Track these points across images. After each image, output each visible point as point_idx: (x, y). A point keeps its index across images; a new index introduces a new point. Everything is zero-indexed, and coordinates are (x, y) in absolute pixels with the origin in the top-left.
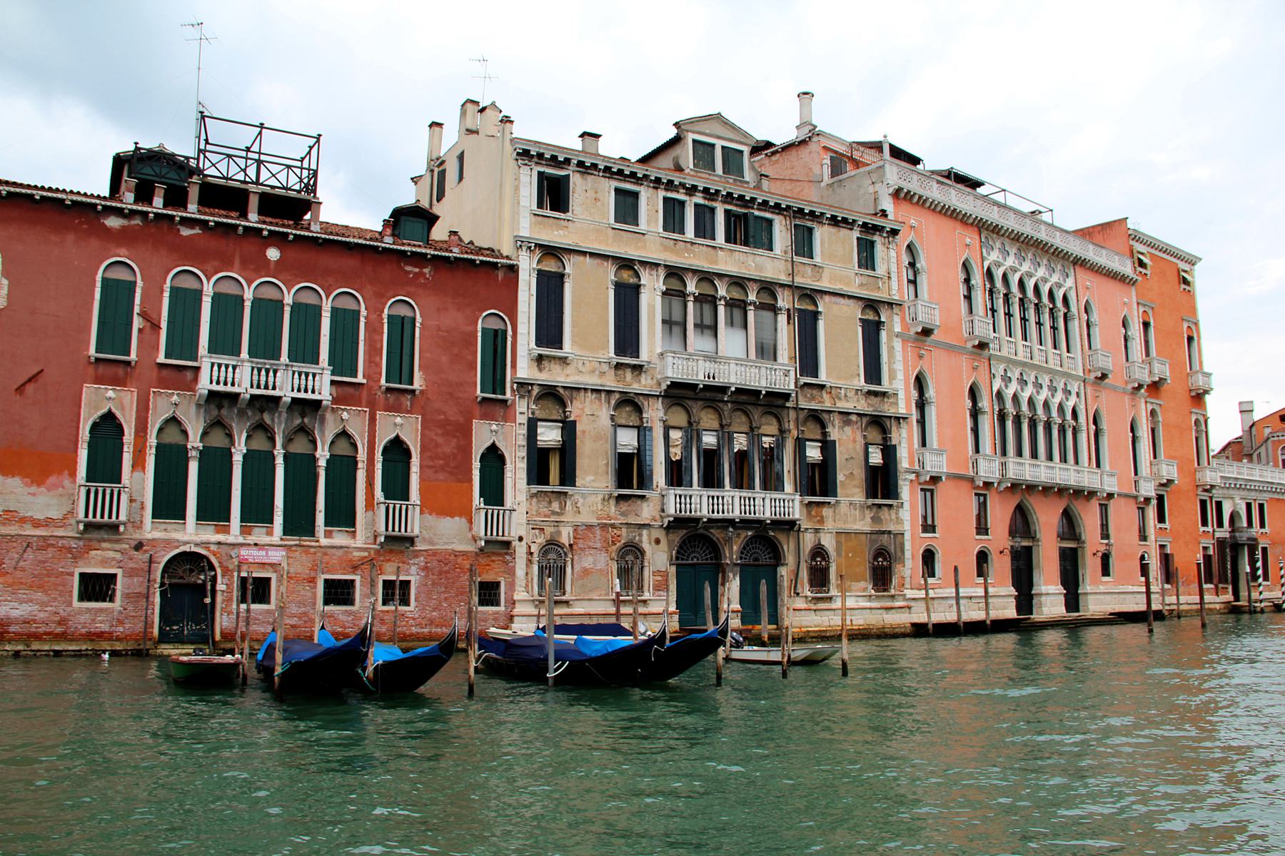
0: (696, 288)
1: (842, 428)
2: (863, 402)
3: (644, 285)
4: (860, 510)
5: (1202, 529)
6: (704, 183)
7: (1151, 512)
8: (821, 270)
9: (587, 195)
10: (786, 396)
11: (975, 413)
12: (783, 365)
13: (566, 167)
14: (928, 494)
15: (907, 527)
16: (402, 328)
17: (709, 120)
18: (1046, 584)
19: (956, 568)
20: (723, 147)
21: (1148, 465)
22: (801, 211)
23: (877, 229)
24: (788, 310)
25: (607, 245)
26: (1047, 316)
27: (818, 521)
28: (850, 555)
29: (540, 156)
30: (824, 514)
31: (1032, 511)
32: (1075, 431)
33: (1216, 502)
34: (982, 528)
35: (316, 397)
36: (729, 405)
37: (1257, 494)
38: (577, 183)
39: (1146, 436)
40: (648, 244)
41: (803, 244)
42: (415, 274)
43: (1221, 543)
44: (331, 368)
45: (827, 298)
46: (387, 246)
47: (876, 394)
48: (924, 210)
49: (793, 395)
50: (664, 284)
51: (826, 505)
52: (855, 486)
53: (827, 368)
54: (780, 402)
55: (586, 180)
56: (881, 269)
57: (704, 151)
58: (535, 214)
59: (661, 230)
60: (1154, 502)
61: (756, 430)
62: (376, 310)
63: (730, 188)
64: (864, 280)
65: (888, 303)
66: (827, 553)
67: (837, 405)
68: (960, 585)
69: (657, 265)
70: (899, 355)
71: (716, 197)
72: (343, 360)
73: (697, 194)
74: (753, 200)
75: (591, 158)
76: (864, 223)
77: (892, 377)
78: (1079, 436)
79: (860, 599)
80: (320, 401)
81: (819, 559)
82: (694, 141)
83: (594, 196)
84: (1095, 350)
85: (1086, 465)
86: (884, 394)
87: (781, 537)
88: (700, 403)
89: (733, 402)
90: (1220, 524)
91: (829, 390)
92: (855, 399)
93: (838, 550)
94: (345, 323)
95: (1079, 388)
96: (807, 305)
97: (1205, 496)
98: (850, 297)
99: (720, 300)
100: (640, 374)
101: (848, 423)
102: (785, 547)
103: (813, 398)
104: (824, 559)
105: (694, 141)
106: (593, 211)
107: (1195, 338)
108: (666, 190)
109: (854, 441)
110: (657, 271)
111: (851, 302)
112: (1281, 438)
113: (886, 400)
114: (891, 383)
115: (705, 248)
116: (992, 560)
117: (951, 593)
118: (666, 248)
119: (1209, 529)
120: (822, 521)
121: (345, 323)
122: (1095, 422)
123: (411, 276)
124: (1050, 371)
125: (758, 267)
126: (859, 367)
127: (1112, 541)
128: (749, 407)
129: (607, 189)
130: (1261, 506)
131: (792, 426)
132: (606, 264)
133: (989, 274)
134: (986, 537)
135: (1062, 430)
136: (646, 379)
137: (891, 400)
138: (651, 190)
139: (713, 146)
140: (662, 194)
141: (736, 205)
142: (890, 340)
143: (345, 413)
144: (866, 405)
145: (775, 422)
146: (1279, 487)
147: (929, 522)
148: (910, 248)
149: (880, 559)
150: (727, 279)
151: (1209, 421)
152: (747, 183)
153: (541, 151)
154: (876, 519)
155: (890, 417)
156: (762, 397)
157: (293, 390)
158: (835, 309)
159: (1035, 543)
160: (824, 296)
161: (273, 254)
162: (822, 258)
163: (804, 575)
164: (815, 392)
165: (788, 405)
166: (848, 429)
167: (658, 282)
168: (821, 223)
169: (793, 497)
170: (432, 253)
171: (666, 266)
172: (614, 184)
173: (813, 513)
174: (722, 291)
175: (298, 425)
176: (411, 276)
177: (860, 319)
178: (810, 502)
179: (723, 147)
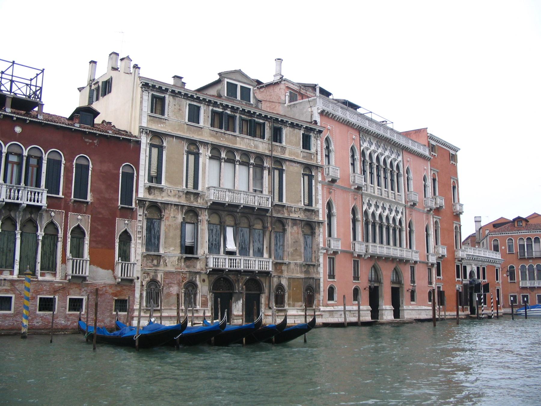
0: (225, 156)
1: (292, 227)
2: (302, 214)
3: (201, 154)
4: (300, 267)
5: (457, 279)
7: (434, 271)
9: (176, 107)
10: (267, 210)
11: (354, 221)
12: (266, 195)
13: (166, 93)
14: (331, 260)
15: (322, 276)
16: (82, 170)
17: (235, 72)
18: (385, 305)
19: (344, 296)
20: (241, 86)
21: (433, 247)
22: (277, 119)
23: (312, 130)
24: (269, 168)
25: (184, 132)
26: (389, 174)
27: (280, 272)
28: (295, 289)
29: (154, 86)
31: (380, 269)
32: (400, 231)
33: (464, 266)
34: (356, 278)
35: (39, 204)
36: (240, 214)
37: (482, 263)
38: (170, 101)
39: (433, 234)
40: (203, 133)
41: (277, 136)
42: (90, 143)
43: (465, 286)
44: (47, 190)
45: (287, 163)
46: (77, 128)
48: (334, 121)
49: (270, 210)
50: (210, 153)
51: (284, 264)
52: (298, 255)
53: (286, 198)
54: (263, 213)
55: (175, 99)
56: (313, 150)
57: (232, 88)
58: (150, 116)
59: (210, 127)
60: (436, 266)
61: (252, 226)
62: (69, 160)
63: (244, 107)
64: (305, 155)
65: (316, 166)
66: (284, 288)
67: (291, 215)
68: (346, 305)
69: (208, 143)
70: (320, 192)
71: (237, 111)
72: (53, 186)
73: (228, 109)
74: (255, 113)
75: (178, 89)
76: (306, 127)
77: (317, 203)
78: (402, 233)
79: (299, 311)
80: (41, 206)
81: (280, 291)
82: (227, 82)
83: (179, 107)
84: (411, 192)
85: (405, 247)
86: (313, 211)
87: (263, 280)
88: (226, 213)
89: (241, 213)
90: (465, 277)
91: (286, 208)
92: (299, 213)
93: (289, 286)
94: (54, 165)
95: (403, 210)
96: (278, 166)
97: (458, 263)
98: (298, 163)
99: (237, 162)
100: (198, 197)
103: (279, 212)
104: (282, 291)
105: (227, 82)
106: (177, 115)
107: (456, 187)
108: (213, 106)
109: (298, 233)
110: (207, 146)
111: (298, 165)
112: (493, 235)
114: (316, 205)
115: (230, 136)
116: (360, 292)
117: (342, 308)
118: (212, 136)
119: (460, 279)
120: (282, 272)
121: (54, 165)
122: (410, 227)
123: (88, 144)
124: (390, 201)
125: (256, 147)
126: (301, 197)
127: (415, 284)
128: (249, 215)
129: (185, 105)
130: (484, 269)
131: (269, 225)
132: (183, 142)
133: (363, 154)
134: (358, 281)
135: (394, 230)
136: (200, 200)
138: (206, 106)
140: (211, 108)
141: (246, 115)
142: (316, 184)
143: (53, 213)
144: (304, 216)
145: (261, 223)
146: (492, 260)
147: (332, 274)
148: (327, 140)
149: (309, 291)
150: (240, 152)
151: (461, 227)
152: (252, 105)
153: (154, 84)
156: (255, 210)
157: (27, 200)
158: (291, 168)
159: (380, 285)
160: (286, 162)
161: (18, 130)
162: (286, 143)
165: (267, 215)
166: (295, 228)
167: (208, 152)
168: (286, 126)
169: (269, 260)
170: (99, 133)
171: (212, 144)
172: (188, 102)
173: (278, 268)
174: (238, 158)
175: (29, 218)
176: (88, 144)
177: (302, 174)
178: (276, 263)
179: (241, 86)
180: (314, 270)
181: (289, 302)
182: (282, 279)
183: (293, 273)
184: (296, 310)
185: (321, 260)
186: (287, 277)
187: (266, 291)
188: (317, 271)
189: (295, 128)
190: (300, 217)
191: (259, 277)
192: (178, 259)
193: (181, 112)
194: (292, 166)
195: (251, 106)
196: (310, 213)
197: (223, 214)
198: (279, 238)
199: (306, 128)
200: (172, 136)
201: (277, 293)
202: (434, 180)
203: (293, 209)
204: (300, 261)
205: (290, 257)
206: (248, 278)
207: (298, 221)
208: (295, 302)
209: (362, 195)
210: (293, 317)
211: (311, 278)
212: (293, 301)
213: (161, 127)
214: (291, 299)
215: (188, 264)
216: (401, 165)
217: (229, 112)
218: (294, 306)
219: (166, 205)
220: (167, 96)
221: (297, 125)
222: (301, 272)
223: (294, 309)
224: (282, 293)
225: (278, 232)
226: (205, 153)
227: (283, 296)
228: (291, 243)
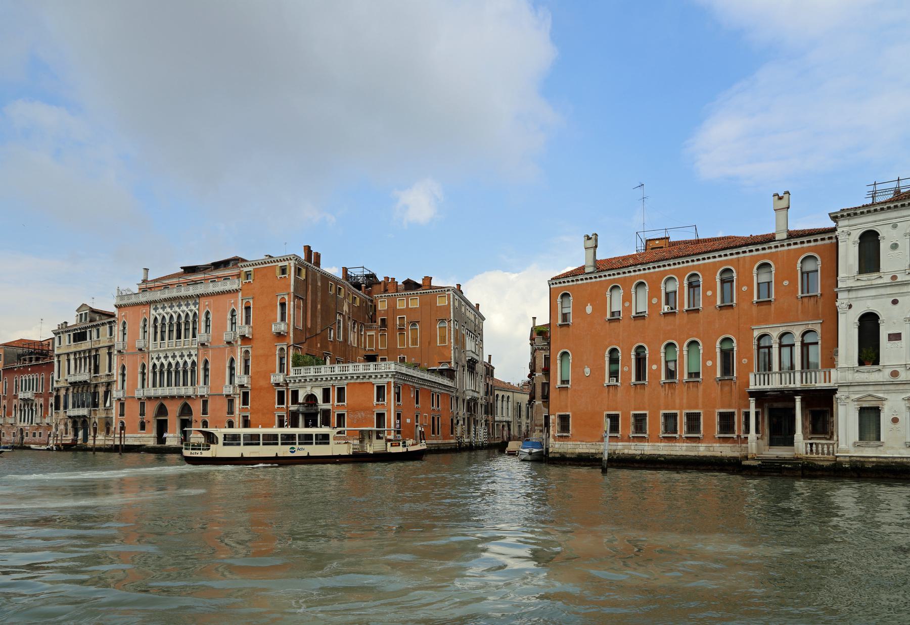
45: (101, 349)
101: (103, 386)
118: (75, 347)
120: (96, 415)
139: (82, 314)
154: (107, 414)
164: (96, 378)
172: (67, 334)
202: (248, 309)
216: (197, 312)
226: (72, 357)
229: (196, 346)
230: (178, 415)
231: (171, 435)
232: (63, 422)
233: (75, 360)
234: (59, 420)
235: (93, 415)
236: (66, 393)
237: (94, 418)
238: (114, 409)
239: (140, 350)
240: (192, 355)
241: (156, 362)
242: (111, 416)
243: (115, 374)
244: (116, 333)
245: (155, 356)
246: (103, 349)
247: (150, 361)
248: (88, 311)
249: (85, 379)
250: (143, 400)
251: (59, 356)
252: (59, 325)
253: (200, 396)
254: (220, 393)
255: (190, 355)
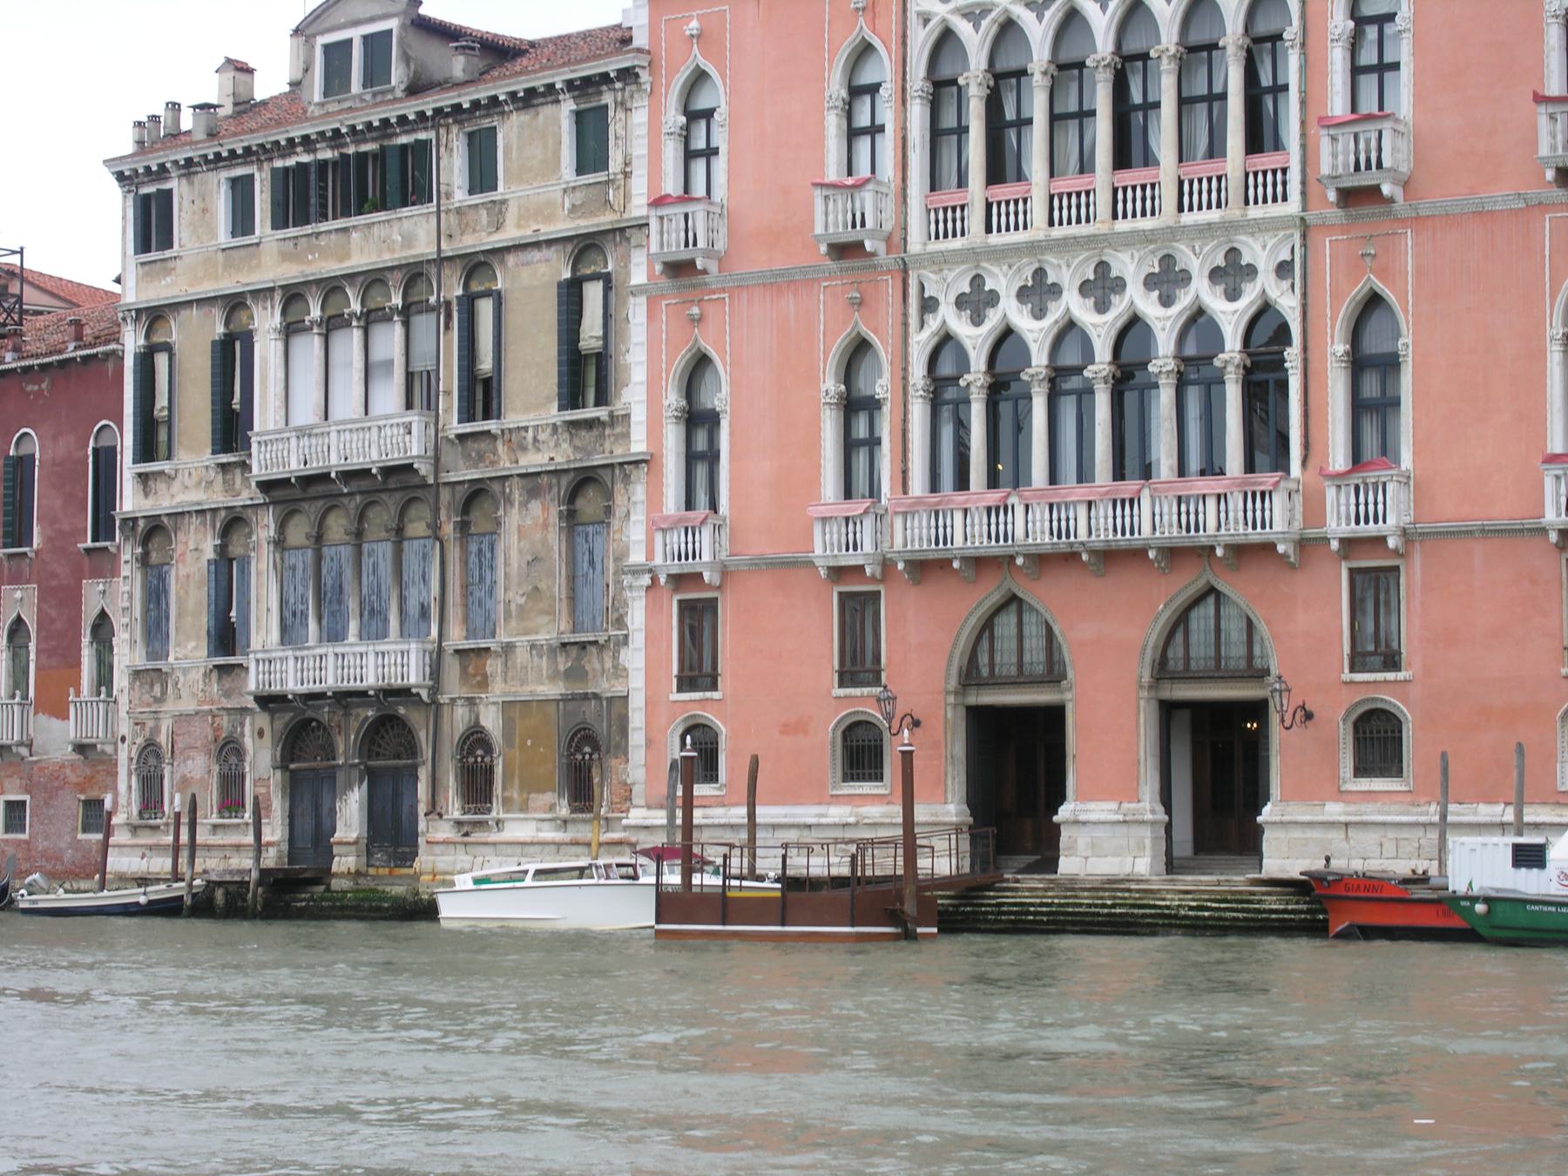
1: (524, 505)
2: (565, 446)
4: (548, 658)
6: (314, 126)
8: (504, 207)
22: (457, 108)
25: (217, 279)
28: (529, 743)
30: (488, 669)
36: (358, 498)
45: (511, 260)
47: (590, 424)
56: (615, 163)
67: (521, 463)
71: (343, 141)
74: (385, 122)
79: (546, 825)
81: (480, 752)
88: (320, 503)
89: (361, 493)
92: (552, 444)
98: (550, 243)
101: (533, 493)
102: (422, 735)
103: (481, 457)
109: (545, 526)
110: (272, 299)
113: (608, 431)
115: (333, 237)
118: (285, 257)
120: (484, 684)
137: (618, 430)
139: (349, 42)
144: (570, 450)
152: (392, 90)
155: (611, 466)
158: (525, 273)
163: (451, 781)
164: (483, 445)
166: (536, 507)
167: (272, 314)
168: (503, 113)
172: (224, 175)
173: (471, 670)
180: (602, 662)
181: (507, 794)
182: (482, 708)
183: (523, 682)
184: (533, 825)
185: (636, 616)
186: (500, 700)
187: (427, 753)
188: (615, 667)
189: (538, 105)
190: (559, 459)
191: (406, 707)
192: (205, 675)
193: (208, 215)
194: (528, 264)
195: (390, 97)
196: (595, 432)
197: (313, 509)
198: (488, 555)
199: (570, 84)
200: (189, 303)
201: (471, 760)
203: (530, 434)
204: (546, 635)
205: (513, 623)
206: (370, 713)
207: (545, 479)
208: (529, 793)
209: (905, 271)
210: (518, 849)
211: (585, 697)
212: (522, 789)
213: (168, 286)
214: (516, 781)
215: (227, 686)
217: (327, 154)
218: (524, 808)
219: (177, 516)
220: (172, 184)
221: (531, 92)
222: (553, 677)
223: (527, 819)
224: (487, 759)
225: (484, 535)
226: (266, 322)
227: (490, 771)
228: (519, 566)
229: (1293, 206)
230: (1146, 678)
231: (1100, 810)
232: (202, 732)
233: (290, 330)
234: (166, 725)
235: (453, 687)
236: (222, 550)
237: (471, 702)
238: (638, 640)
239: (845, 251)
240: (1251, 271)
241: (962, 327)
242: (607, 687)
243: (639, 415)
244: (640, 149)
245: (948, 285)
246: (536, 255)
247: (913, 320)
248: (393, 24)
249: (396, 458)
250: (873, 579)
251: (154, 316)
252: (139, 124)
253: (1342, 541)
254: (1503, 512)
255: (1232, 274)
